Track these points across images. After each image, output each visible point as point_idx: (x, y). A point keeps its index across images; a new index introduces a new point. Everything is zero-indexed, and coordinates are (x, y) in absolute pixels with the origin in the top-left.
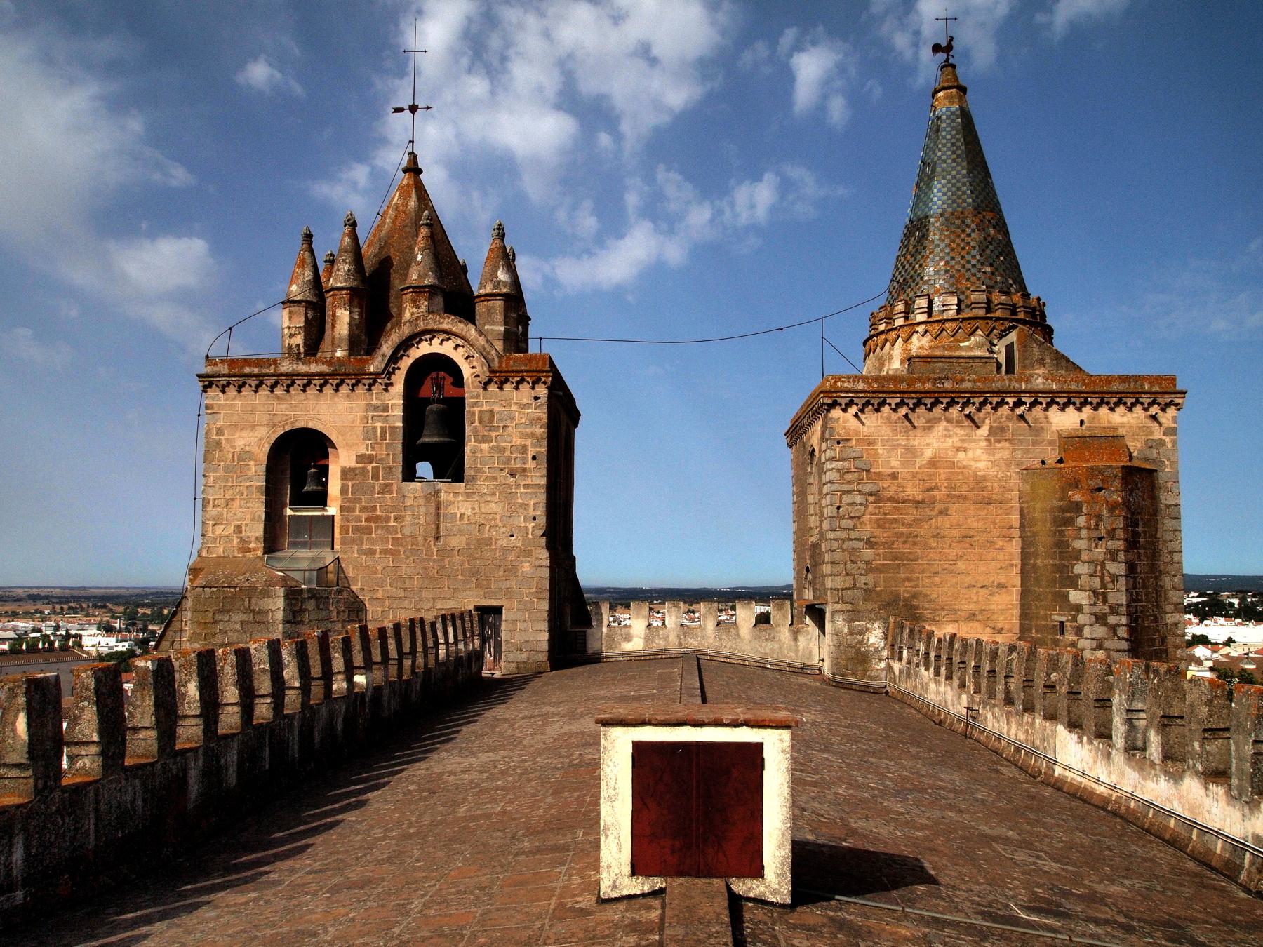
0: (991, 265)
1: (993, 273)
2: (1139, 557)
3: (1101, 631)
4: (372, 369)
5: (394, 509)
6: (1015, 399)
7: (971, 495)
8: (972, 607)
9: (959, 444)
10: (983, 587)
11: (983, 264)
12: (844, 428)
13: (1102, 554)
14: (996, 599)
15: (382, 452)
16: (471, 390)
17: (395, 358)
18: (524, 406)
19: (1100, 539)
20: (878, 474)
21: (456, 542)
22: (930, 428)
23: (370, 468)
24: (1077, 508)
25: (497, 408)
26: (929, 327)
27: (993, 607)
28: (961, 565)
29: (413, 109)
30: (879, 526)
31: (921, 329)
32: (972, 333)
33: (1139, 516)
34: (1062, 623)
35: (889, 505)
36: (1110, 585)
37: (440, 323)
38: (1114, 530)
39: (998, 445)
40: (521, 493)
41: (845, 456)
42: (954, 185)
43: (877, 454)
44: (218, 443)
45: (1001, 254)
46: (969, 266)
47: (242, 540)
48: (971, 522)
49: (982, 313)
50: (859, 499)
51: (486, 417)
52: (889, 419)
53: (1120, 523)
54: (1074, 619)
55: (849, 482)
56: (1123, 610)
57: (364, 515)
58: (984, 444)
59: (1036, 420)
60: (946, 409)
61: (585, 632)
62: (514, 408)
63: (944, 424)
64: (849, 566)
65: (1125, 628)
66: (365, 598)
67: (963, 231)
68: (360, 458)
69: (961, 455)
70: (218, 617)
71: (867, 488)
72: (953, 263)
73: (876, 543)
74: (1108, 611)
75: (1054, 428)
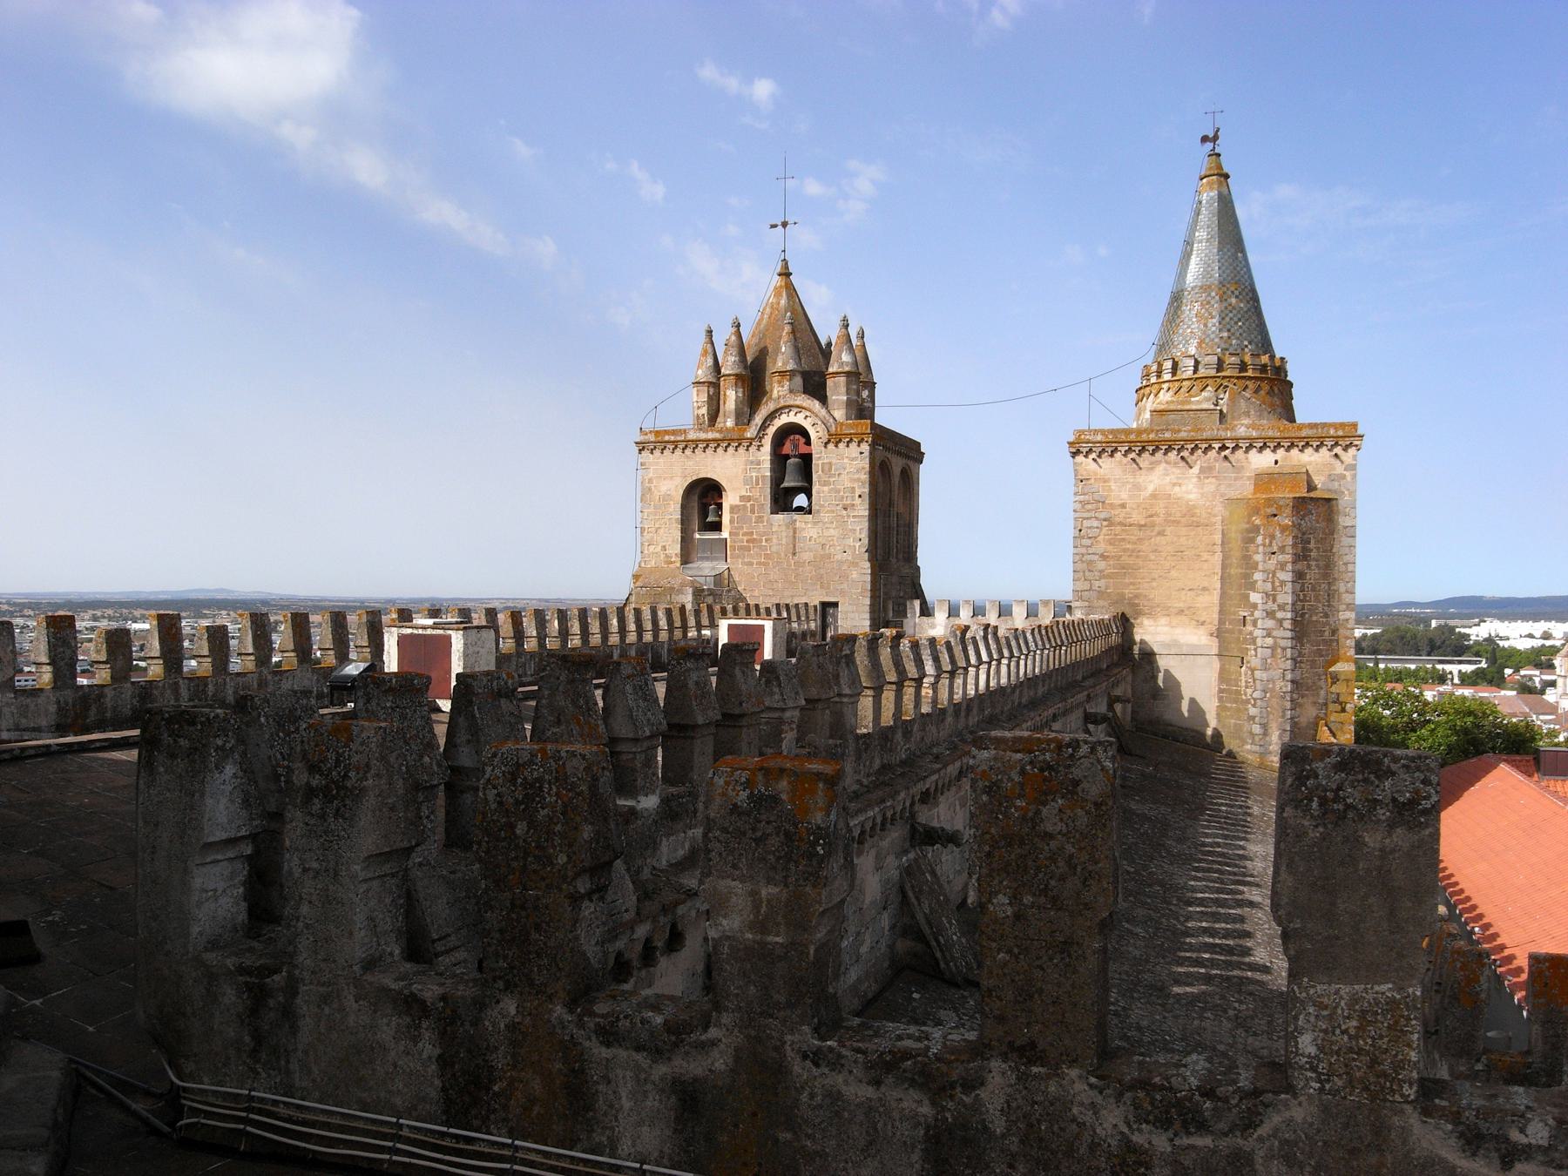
0: (1229, 330)
1: (1229, 338)
2: (1309, 567)
3: (1270, 623)
4: (749, 435)
5: (765, 533)
7: (1183, 520)
8: (1181, 605)
9: (1175, 481)
12: (1086, 470)
14: (1200, 598)
16: (816, 448)
17: (764, 427)
18: (853, 459)
19: (1274, 553)
20: (1111, 505)
21: (807, 556)
22: (1152, 469)
23: (748, 504)
24: (1256, 529)
25: (834, 461)
26: (1171, 385)
27: (1198, 605)
28: (1174, 573)
29: (785, 225)
30: (1111, 544)
33: (1311, 536)
36: (1279, 589)
39: (1207, 481)
43: (1110, 490)
44: (650, 489)
45: (1240, 320)
47: (667, 556)
48: (1183, 540)
50: (1096, 523)
51: (826, 468)
52: (1120, 462)
53: (1290, 541)
56: (1289, 607)
57: (745, 538)
58: (1195, 480)
59: (1238, 461)
60: (1165, 454)
62: (846, 461)
63: (1164, 465)
64: (1087, 573)
68: (742, 498)
69: (1177, 489)
71: (1102, 516)
73: (1108, 557)
75: (1253, 466)
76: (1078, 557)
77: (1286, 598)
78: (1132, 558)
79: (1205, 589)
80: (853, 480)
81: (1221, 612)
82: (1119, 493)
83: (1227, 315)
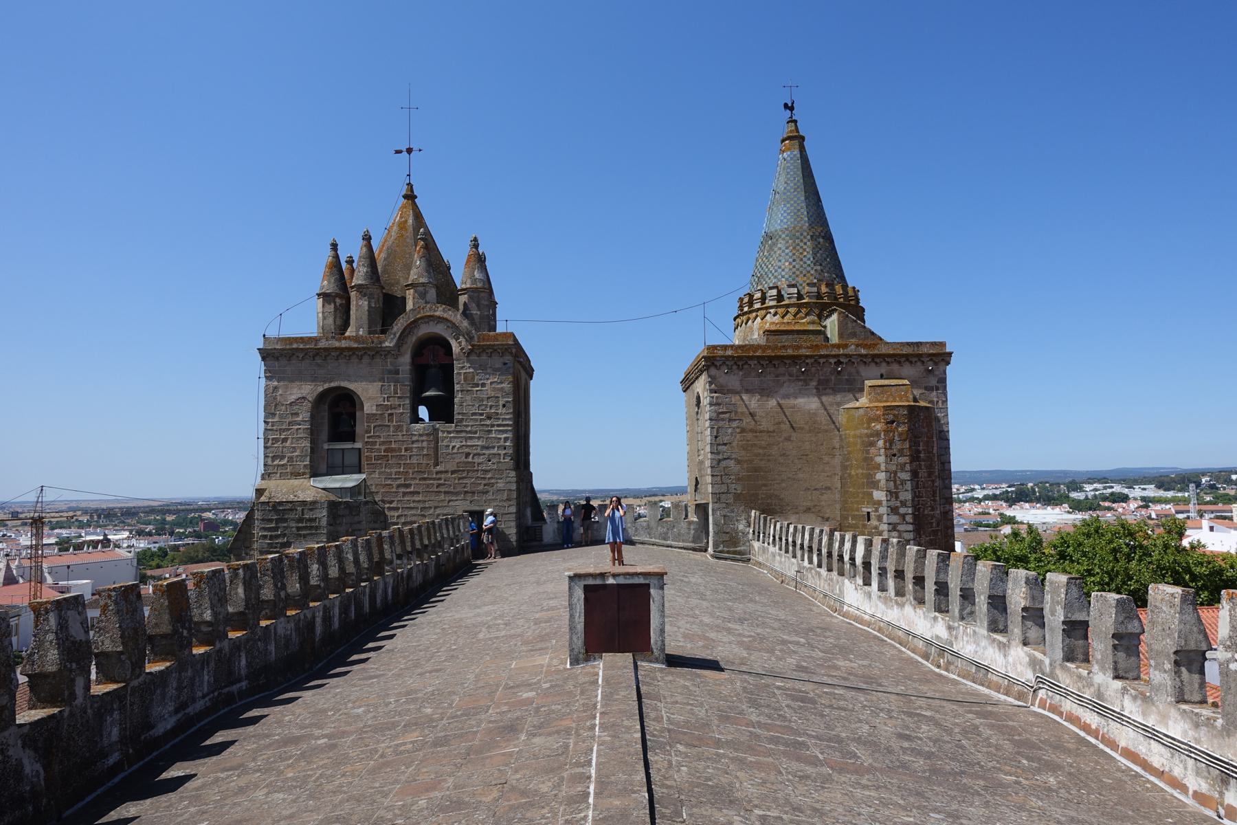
0: (821, 265)
3: (895, 519)
6: (836, 360)
10: (815, 489)
11: (815, 264)
13: (895, 466)
14: (825, 497)
19: (894, 455)
24: (877, 434)
27: (823, 503)
29: (409, 151)
31: (772, 311)
34: (868, 513)
36: (900, 487)
37: (435, 311)
40: (496, 430)
42: (795, 207)
45: (827, 256)
46: (805, 266)
54: (877, 510)
55: (723, 420)
56: (909, 504)
57: (383, 448)
61: (541, 526)
65: (911, 516)
72: (794, 263)
74: (899, 504)
76: (715, 462)
77: (906, 496)
78: (763, 462)
79: (828, 488)
81: (843, 509)
83: (818, 252)
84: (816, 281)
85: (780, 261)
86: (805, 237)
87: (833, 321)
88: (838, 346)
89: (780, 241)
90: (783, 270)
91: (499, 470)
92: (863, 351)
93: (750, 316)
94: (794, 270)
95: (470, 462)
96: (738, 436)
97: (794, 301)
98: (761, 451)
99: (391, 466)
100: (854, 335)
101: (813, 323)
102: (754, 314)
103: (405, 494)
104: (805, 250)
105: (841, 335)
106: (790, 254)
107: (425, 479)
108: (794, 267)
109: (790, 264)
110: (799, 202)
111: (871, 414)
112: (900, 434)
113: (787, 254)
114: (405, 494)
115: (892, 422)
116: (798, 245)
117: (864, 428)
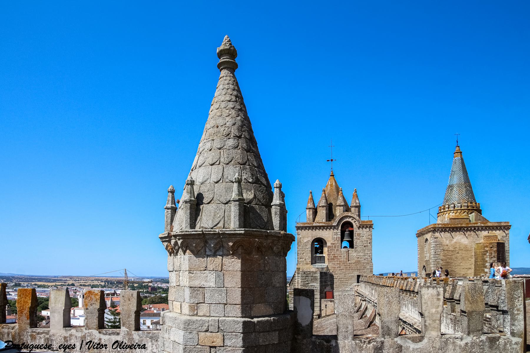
0: (468, 196)
1: (469, 198)
11: (466, 196)
15: (336, 242)
19: (492, 258)
20: (444, 245)
24: (487, 251)
30: (444, 256)
31: (452, 211)
32: (464, 213)
35: (446, 251)
38: (495, 256)
41: (437, 241)
43: (443, 241)
45: (470, 193)
46: (463, 196)
49: (466, 208)
50: (440, 250)
55: (438, 247)
57: (333, 256)
66: (333, 273)
67: (462, 188)
70: (306, 278)
71: (441, 248)
72: (459, 196)
73: (443, 260)
78: (450, 260)
80: (367, 238)
82: (446, 242)
84: (466, 202)
85: (454, 195)
86: (463, 187)
87: (473, 215)
88: (475, 224)
89: (454, 188)
90: (456, 198)
91: (368, 263)
92: (483, 225)
93: (444, 213)
94: (459, 198)
95: (359, 261)
96: (442, 252)
97: (459, 208)
98: (449, 257)
99: (335, 262)
100: (480, 220)
101: (466, 215)
102: (446, 212)
103: (339, 270)
104: (463, 191)
105: (475, 220)
106: (458, 193)
107: (345, 265)
108: (459, 197)
109: (458, 196)
110: (460, 175)
111: (485, 245)
112: (494, 251)
113: (457, 193)
114: (339, 270)
115: (492, 247)
116: (461, 189)
117: (482, 250)
